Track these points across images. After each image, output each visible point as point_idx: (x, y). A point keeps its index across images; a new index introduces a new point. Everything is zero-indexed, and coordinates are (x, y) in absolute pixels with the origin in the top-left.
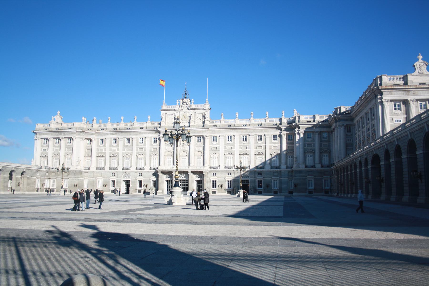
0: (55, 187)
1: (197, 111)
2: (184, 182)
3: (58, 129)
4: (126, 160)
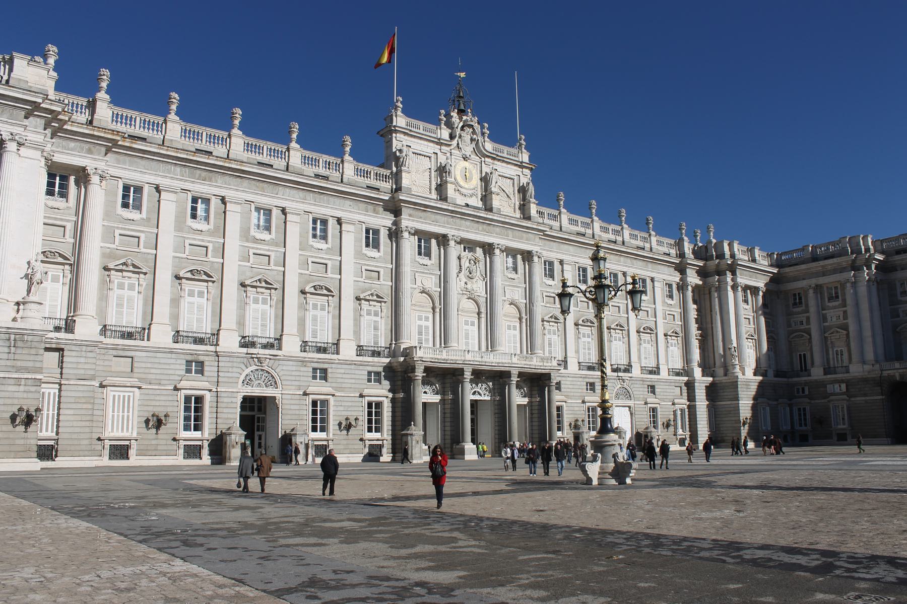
4: (253, 306)
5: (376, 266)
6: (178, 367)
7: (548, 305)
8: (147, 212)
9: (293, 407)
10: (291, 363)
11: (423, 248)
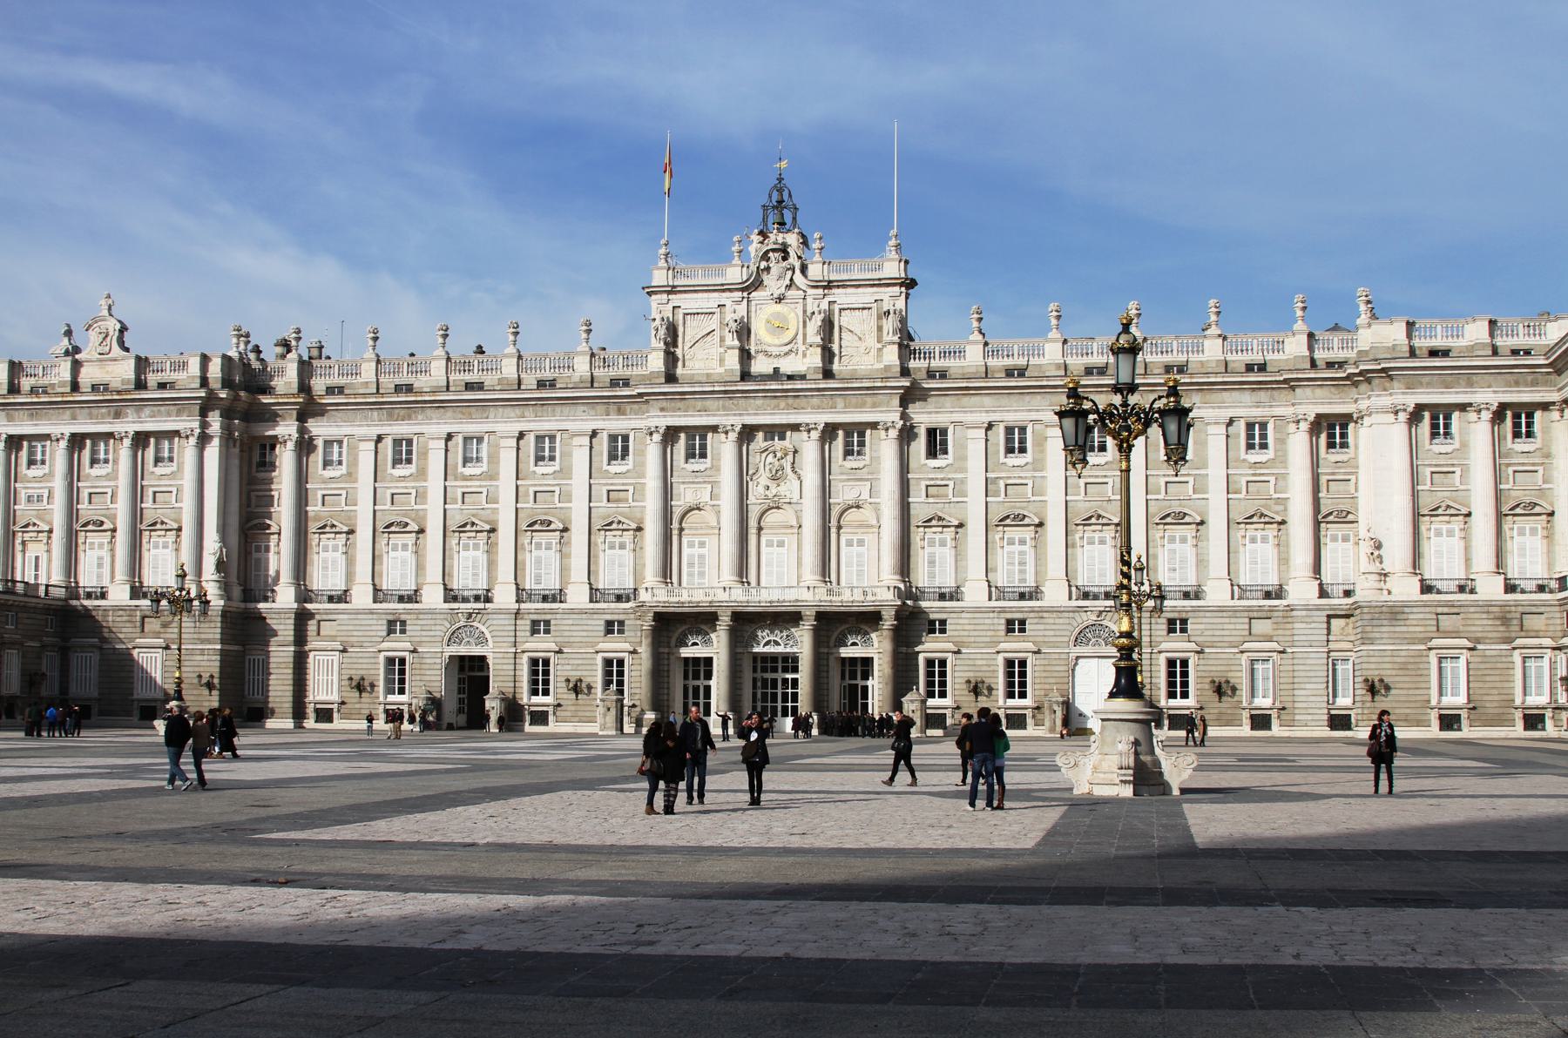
0: (95, 694)
1: (841, 297)
2: (775, 670)
3: (106, 390)
5: (623, 484)
6: (380, 628)
7: (931, 500)
8: (348, 465)
9: (505, 667)
10: (503, 616)
11: (697, 447)
